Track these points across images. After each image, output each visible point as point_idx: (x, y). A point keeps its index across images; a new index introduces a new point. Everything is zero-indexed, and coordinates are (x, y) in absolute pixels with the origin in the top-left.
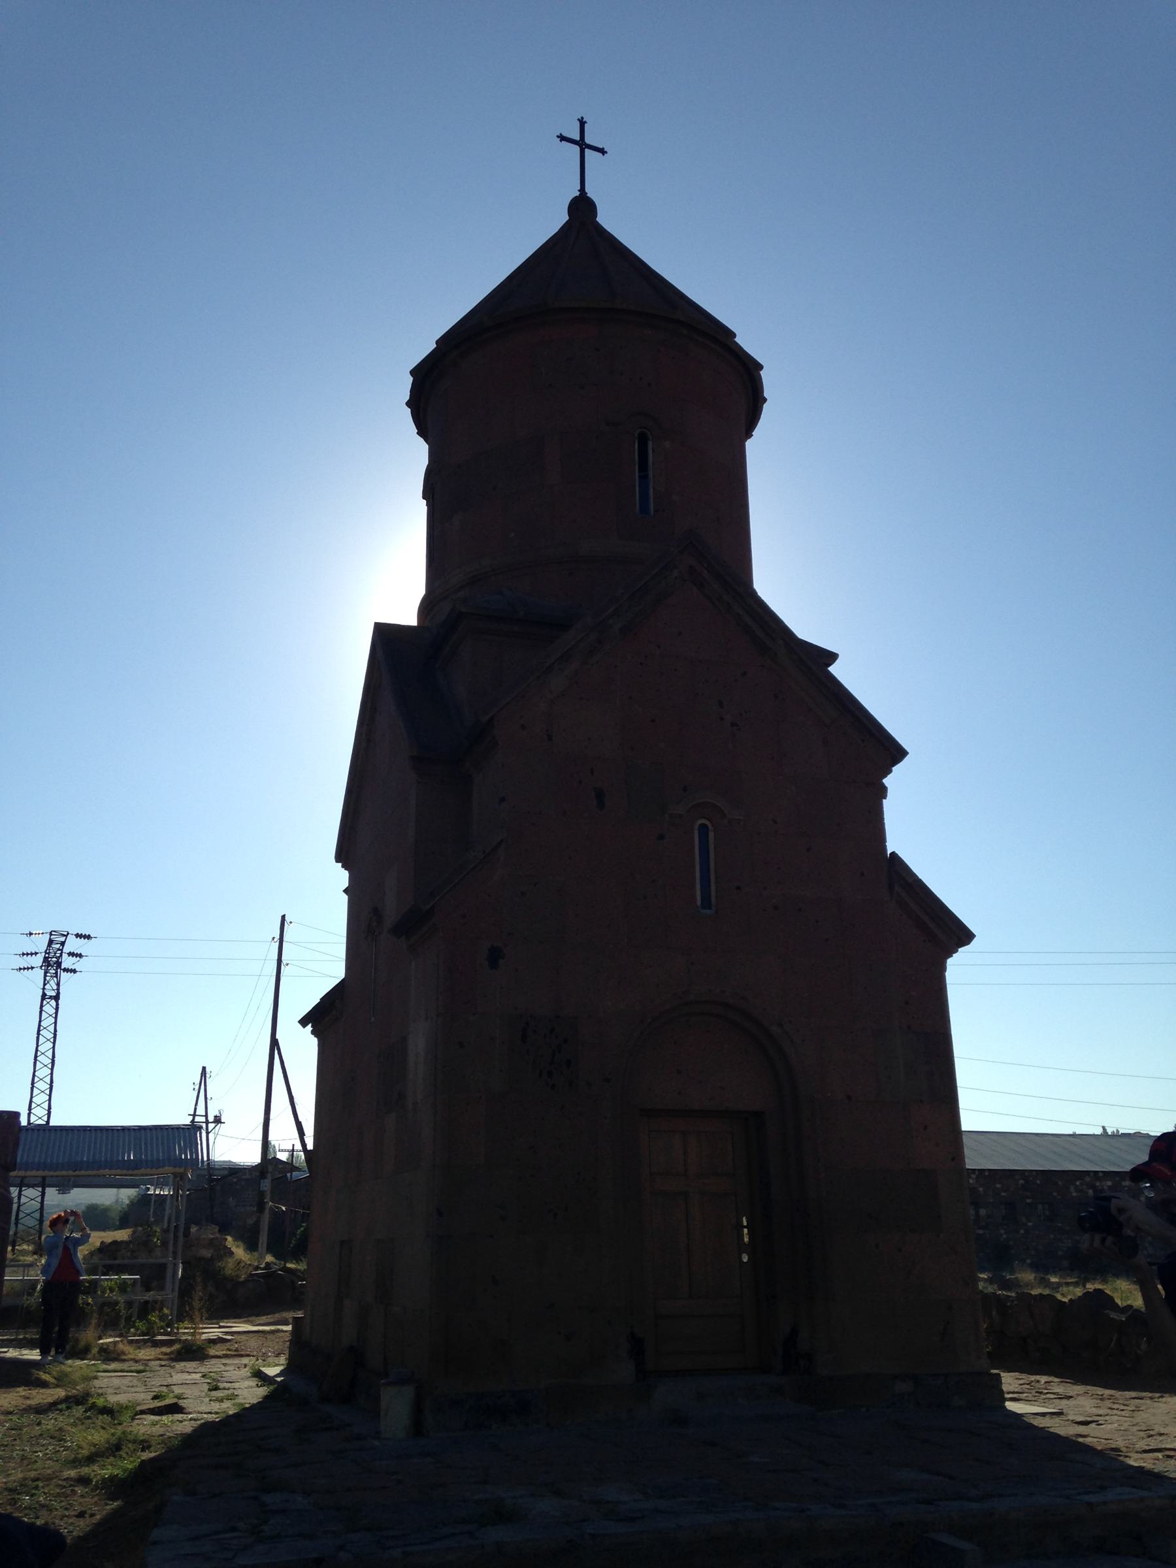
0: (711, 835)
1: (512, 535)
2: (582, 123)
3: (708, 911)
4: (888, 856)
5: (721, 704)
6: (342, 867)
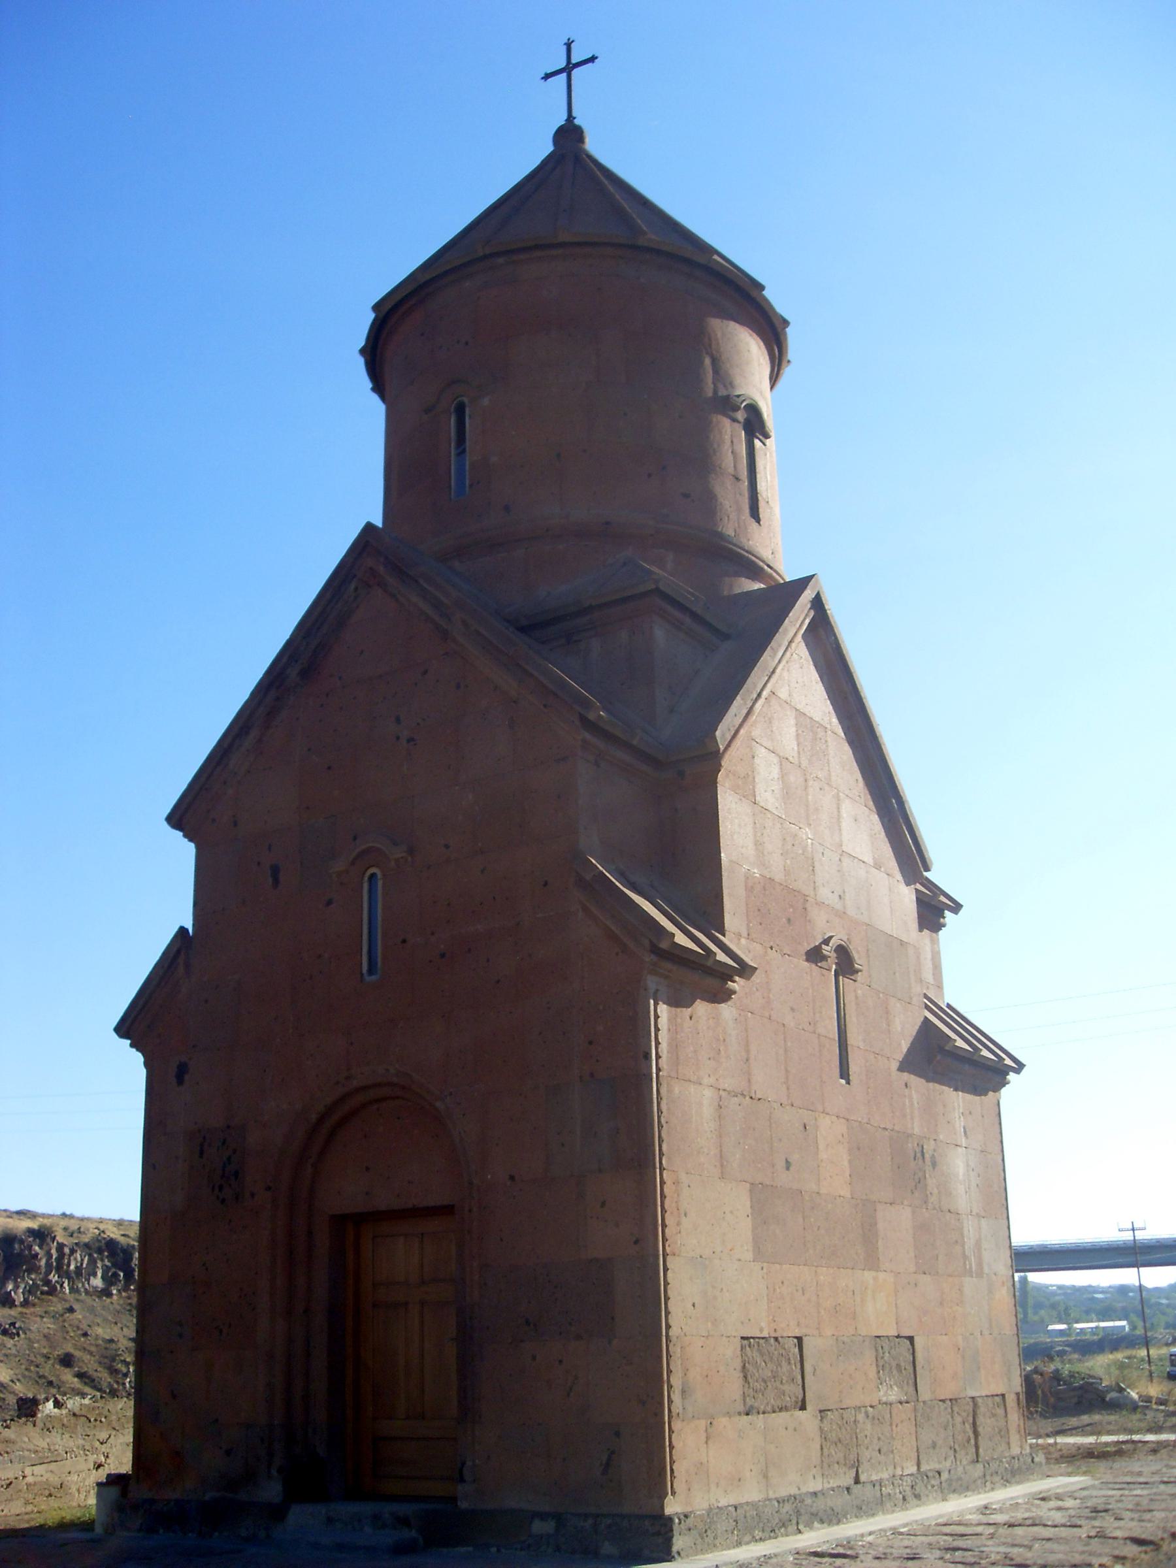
0: (380, 883)
3: (373, 978)
5: (398, 720)
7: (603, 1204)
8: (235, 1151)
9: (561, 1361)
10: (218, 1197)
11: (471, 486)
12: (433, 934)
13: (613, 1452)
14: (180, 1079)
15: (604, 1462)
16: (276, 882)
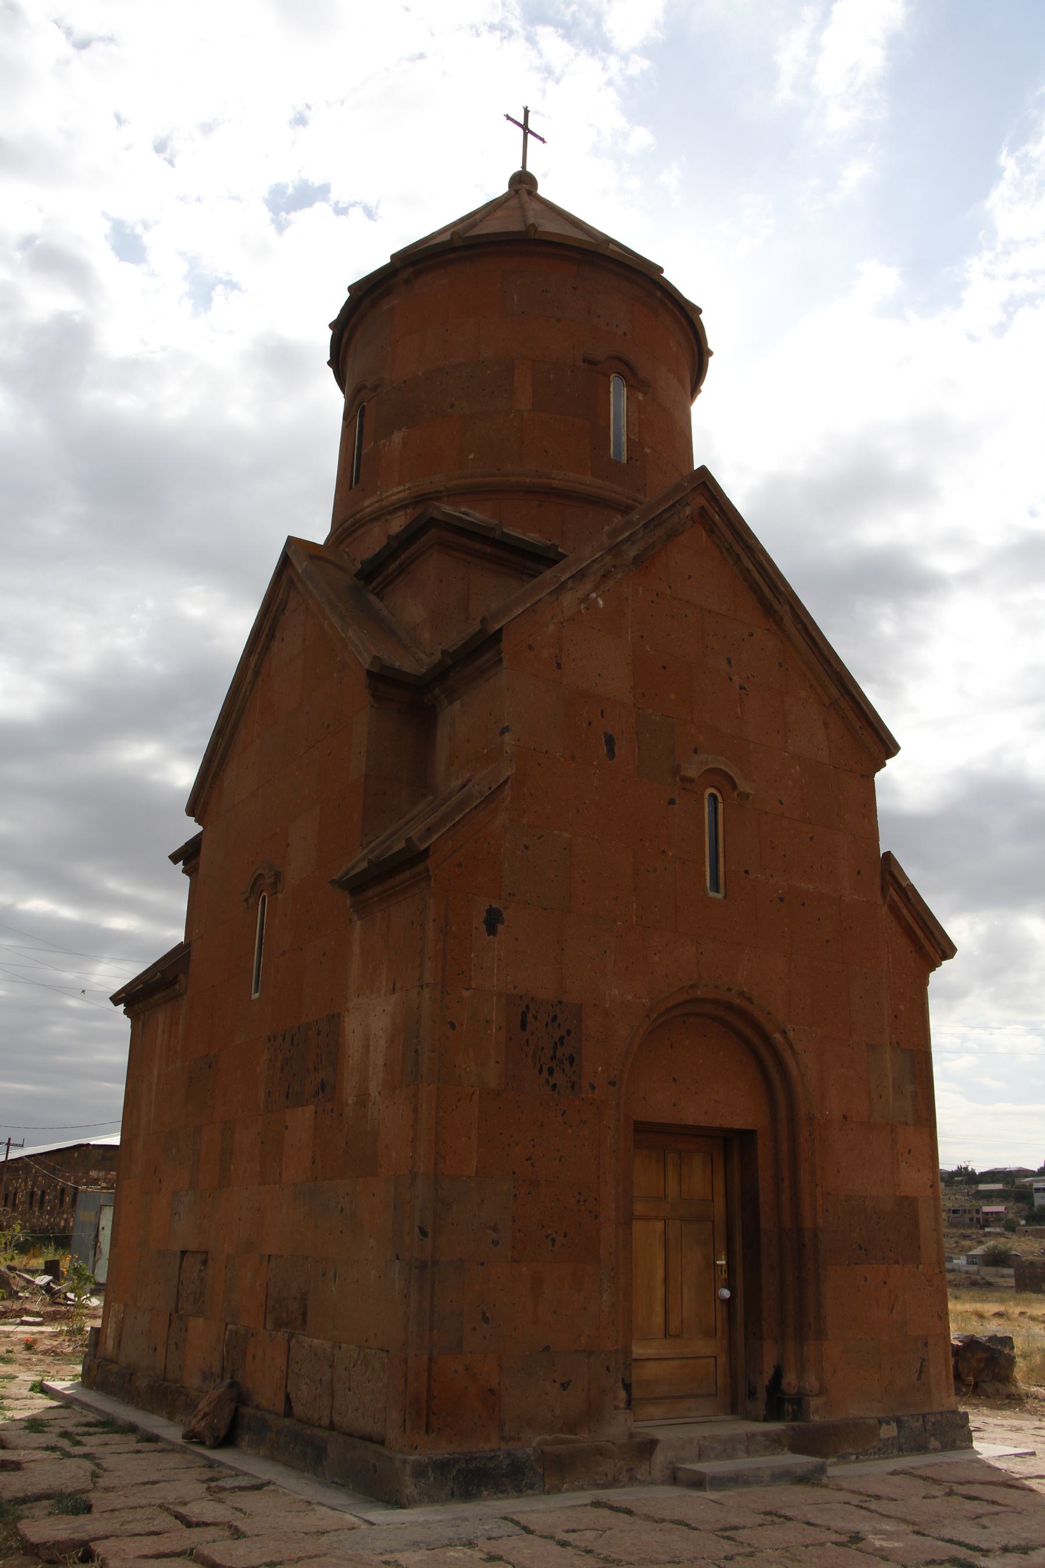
0: (720, 807)
1: (471, 456)
2: (526, 112)
4: (881, 856)
5: (729, 661)
6: (196, 821)
7: (910, 1151)
8: (569, 1032)
9: (885, 1283)
10: (547, 1082)
11: (629, 458)
12: (772, 876)
13: (924, 1360)
14: (491, 929)
15: (918, 1369)
16: (611, 754)
